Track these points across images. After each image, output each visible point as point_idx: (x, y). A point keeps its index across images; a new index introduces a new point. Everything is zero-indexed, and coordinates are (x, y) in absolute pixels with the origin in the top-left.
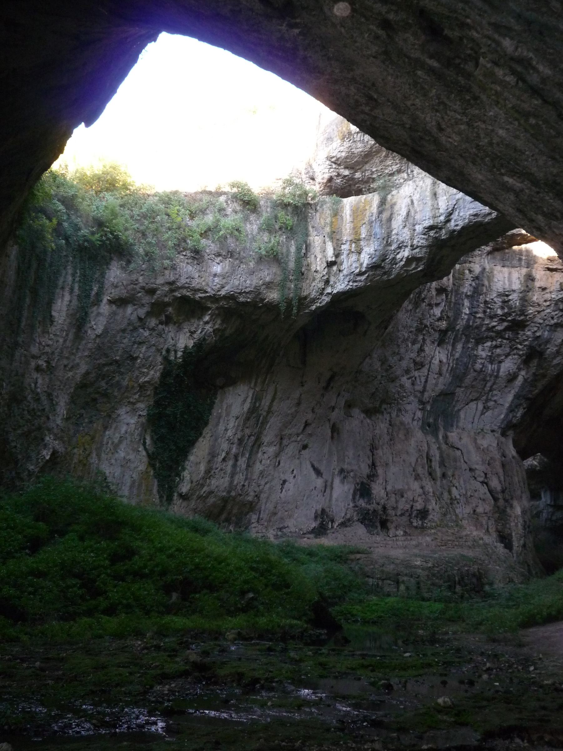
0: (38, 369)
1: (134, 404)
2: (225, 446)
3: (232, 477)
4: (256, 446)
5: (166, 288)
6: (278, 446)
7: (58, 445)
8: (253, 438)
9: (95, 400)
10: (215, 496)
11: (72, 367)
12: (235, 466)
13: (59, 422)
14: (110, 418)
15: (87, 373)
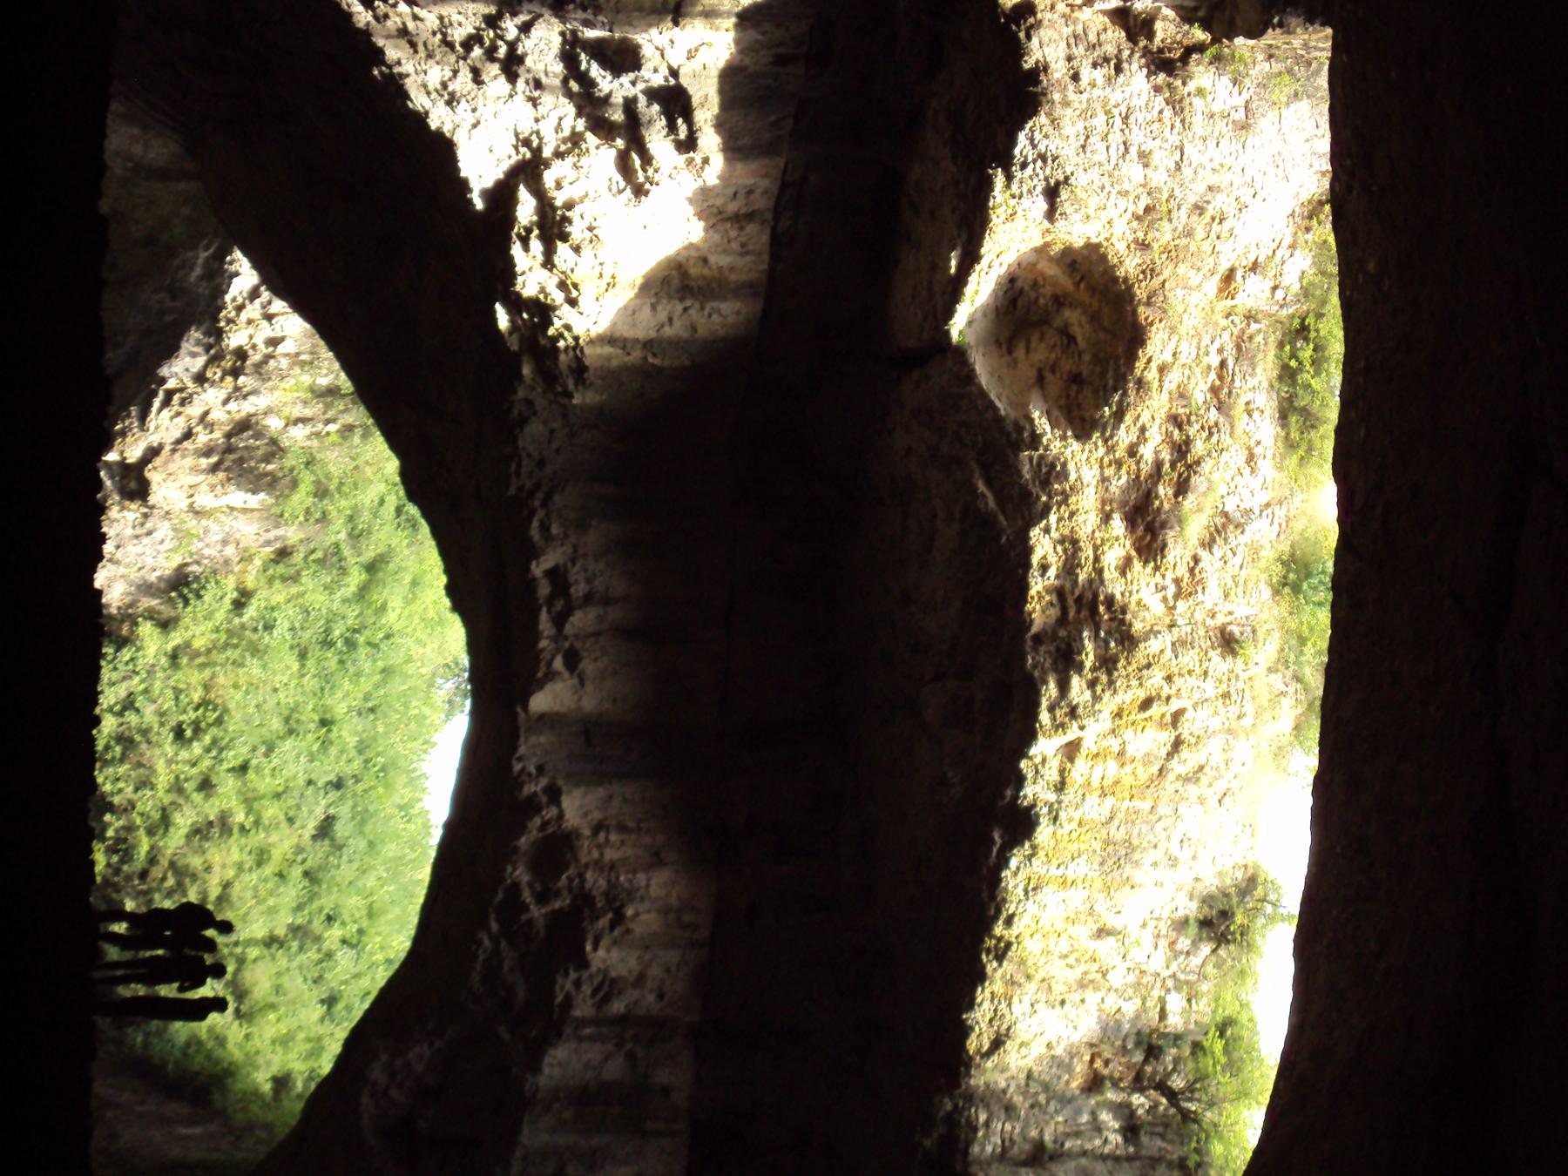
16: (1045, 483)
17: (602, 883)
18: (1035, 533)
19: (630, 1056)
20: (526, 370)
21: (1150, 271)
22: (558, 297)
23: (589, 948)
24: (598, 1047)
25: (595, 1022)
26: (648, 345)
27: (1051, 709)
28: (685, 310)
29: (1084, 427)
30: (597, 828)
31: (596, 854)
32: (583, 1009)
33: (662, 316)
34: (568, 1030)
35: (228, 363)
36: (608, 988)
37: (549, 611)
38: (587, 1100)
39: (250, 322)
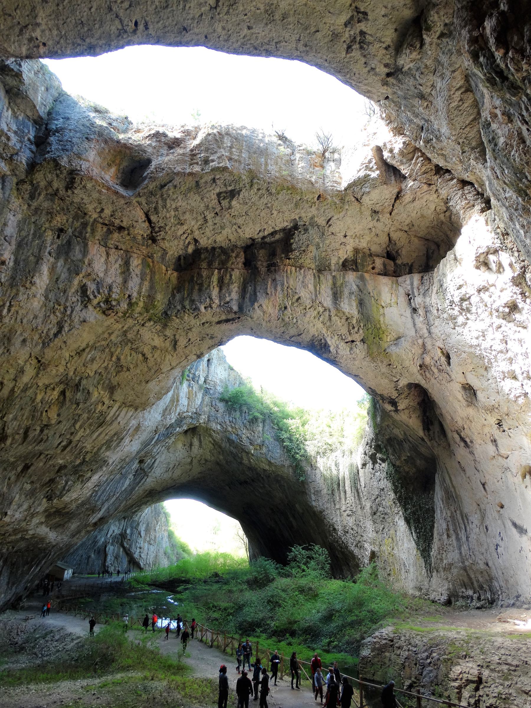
0: (348, 516)
2: (444, 526)
3: (460, 549)
4: (465, 518)
5: (367, 447)
6: (478, 512)
9: (384, 518)
10: (456, 567)
12: (458, 539)
15: (371, 507)
16: (163, 169)
18: (175, 171)
21: (106, 142)
27: (219, 163)
29: (149, 161)
35: (234, 430)
38: (336, 296)
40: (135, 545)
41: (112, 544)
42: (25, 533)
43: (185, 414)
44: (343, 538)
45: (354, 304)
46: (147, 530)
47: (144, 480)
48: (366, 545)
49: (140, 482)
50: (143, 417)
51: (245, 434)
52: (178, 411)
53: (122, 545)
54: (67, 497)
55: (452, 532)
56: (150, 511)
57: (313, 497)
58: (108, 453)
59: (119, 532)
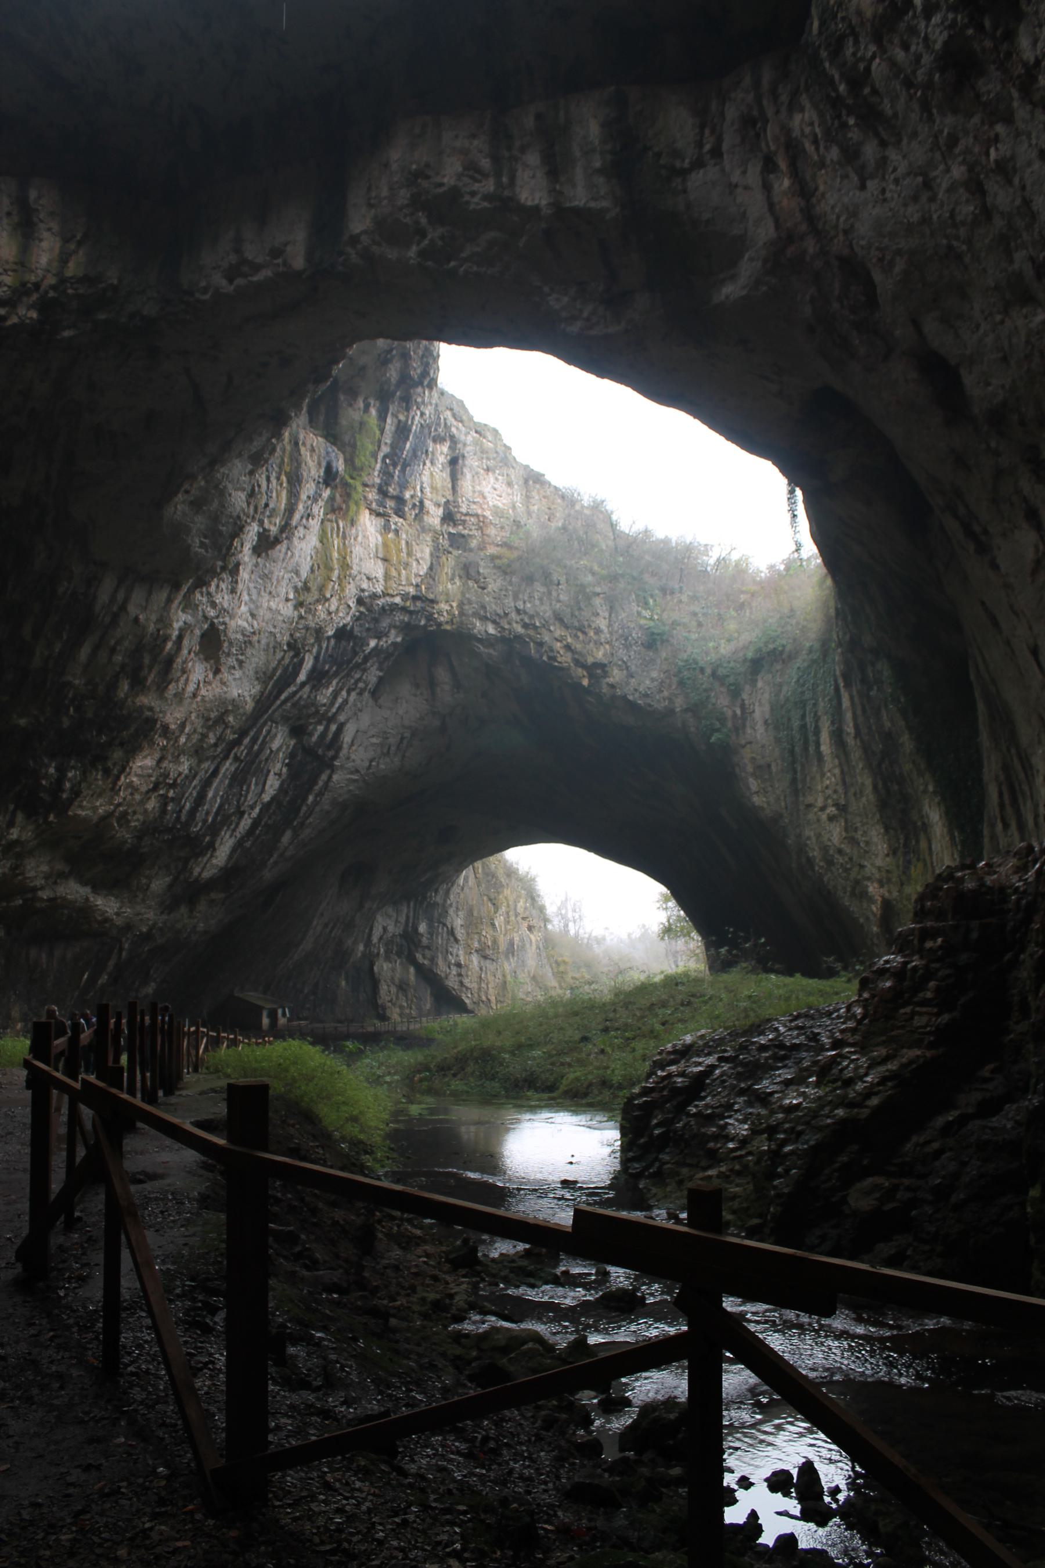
0: (831, 819)
1: (925, 791)
7: (889, 892)
8: (1013, 751)
11: (861, 792)
12: (1021, 827)
13: (879, 862)
14: (926, 827)
15: (875, 787)
17: (403, 192)
19: (523, 150)
20: (102, 316)
22: (35, 296)
23: (441, 190)
24: (519, 173)
25: (498, 175)
26: (66, 241)
28: (41, 221)
30: (370, 206)
31: (385, 202)
32: (489, 186)
33: (45, 235)
34: (506, 193)
35: (531, 632)
36: (472, 169)
37: (251, 275)
38: (555, 169)
39: (509, 623)
40: (445, 959)
41: (388, 958)
42: (30, 896)
43: (380, 602)
44: (825, 879)
45: (600, 180)
46: (473, 923)
47: (324, 777)
48: (873, 889)
49: (314, 781)
50: (214, 605)
51: (555, 638)
52: (351, 590)
53: (413, 961)
54: (81, 807)
55: (1009, 810)
56: (472, 881)
57: (754, 784)
58: (144, 700)
59: (399, 930)
